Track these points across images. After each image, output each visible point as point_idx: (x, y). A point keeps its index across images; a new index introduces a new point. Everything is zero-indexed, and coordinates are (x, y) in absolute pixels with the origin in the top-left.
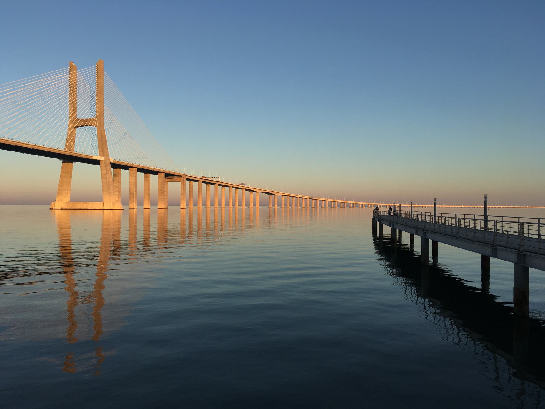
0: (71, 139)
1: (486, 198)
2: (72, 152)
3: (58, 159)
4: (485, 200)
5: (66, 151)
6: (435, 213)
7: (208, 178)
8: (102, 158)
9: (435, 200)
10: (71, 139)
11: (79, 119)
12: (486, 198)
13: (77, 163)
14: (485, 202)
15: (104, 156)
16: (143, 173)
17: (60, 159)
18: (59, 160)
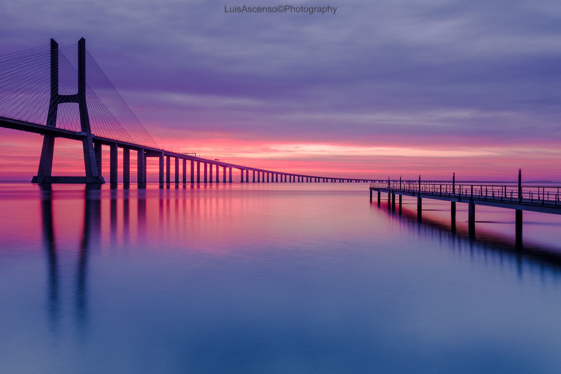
0: (52, 115)
1: (520, 171)
2: (54, 127)
3: (40, 134)
4: (519, 173)
5: (48, 126)
6: (447, 188)
7: (186, 153)
8: (85, 134)
9: (454, 174)
10: (52, 115)
11: (61, 96)
12: (520, 171)
13: (58, 138)
14: (519, 175)
15: (86, 132)
16: (123, 149)
17: (42, 134)
18: (41, 135)
